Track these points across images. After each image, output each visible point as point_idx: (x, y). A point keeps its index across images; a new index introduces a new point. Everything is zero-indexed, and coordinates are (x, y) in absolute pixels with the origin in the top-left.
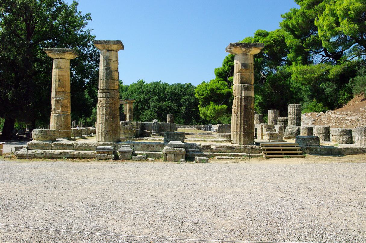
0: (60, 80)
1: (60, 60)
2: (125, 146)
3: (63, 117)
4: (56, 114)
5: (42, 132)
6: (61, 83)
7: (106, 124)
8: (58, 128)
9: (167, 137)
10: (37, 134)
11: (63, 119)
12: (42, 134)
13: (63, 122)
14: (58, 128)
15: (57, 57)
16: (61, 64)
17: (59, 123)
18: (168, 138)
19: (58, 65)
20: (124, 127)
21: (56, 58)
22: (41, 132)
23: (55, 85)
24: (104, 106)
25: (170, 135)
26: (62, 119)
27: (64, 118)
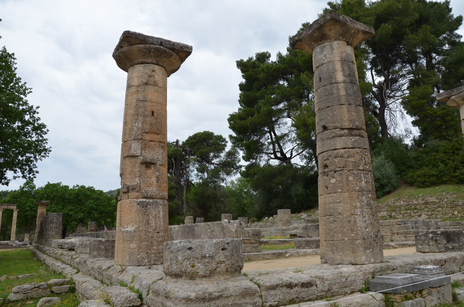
0: (155, 115)
1: (156, 68)
2: (433, 269)
3: (163, 208)
4: (144, 200)
5: (227, 246)
6: (157, 121)
7: (371, 216)
8: (152, 237)
9: (445, 242)
10: (212, 257)
11: (161, 213)
12: (227, 253)
13: (162, 220)
14: (152, 237)
15: (149, 60)
16: (156, 76)
17: (153, 223)
18: (448, 241)
19: (150, 76)
20: (243, 230)
21: (144, 60)
22: (223, 249)
23: (140, 125)
24: (361, 170)
25: (452, 237)
26: (159, 212)
27: (163, 211)
